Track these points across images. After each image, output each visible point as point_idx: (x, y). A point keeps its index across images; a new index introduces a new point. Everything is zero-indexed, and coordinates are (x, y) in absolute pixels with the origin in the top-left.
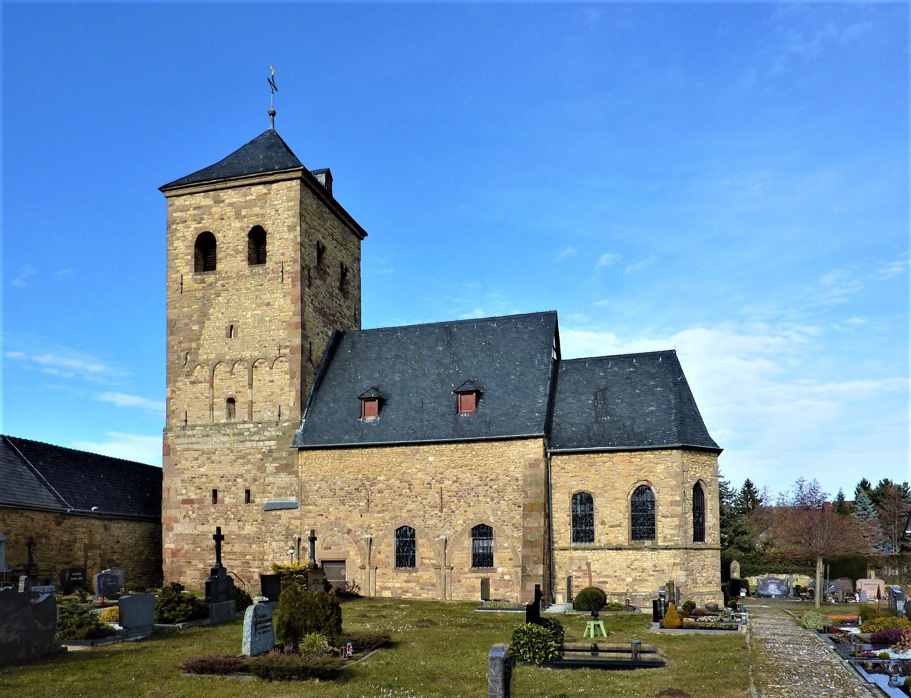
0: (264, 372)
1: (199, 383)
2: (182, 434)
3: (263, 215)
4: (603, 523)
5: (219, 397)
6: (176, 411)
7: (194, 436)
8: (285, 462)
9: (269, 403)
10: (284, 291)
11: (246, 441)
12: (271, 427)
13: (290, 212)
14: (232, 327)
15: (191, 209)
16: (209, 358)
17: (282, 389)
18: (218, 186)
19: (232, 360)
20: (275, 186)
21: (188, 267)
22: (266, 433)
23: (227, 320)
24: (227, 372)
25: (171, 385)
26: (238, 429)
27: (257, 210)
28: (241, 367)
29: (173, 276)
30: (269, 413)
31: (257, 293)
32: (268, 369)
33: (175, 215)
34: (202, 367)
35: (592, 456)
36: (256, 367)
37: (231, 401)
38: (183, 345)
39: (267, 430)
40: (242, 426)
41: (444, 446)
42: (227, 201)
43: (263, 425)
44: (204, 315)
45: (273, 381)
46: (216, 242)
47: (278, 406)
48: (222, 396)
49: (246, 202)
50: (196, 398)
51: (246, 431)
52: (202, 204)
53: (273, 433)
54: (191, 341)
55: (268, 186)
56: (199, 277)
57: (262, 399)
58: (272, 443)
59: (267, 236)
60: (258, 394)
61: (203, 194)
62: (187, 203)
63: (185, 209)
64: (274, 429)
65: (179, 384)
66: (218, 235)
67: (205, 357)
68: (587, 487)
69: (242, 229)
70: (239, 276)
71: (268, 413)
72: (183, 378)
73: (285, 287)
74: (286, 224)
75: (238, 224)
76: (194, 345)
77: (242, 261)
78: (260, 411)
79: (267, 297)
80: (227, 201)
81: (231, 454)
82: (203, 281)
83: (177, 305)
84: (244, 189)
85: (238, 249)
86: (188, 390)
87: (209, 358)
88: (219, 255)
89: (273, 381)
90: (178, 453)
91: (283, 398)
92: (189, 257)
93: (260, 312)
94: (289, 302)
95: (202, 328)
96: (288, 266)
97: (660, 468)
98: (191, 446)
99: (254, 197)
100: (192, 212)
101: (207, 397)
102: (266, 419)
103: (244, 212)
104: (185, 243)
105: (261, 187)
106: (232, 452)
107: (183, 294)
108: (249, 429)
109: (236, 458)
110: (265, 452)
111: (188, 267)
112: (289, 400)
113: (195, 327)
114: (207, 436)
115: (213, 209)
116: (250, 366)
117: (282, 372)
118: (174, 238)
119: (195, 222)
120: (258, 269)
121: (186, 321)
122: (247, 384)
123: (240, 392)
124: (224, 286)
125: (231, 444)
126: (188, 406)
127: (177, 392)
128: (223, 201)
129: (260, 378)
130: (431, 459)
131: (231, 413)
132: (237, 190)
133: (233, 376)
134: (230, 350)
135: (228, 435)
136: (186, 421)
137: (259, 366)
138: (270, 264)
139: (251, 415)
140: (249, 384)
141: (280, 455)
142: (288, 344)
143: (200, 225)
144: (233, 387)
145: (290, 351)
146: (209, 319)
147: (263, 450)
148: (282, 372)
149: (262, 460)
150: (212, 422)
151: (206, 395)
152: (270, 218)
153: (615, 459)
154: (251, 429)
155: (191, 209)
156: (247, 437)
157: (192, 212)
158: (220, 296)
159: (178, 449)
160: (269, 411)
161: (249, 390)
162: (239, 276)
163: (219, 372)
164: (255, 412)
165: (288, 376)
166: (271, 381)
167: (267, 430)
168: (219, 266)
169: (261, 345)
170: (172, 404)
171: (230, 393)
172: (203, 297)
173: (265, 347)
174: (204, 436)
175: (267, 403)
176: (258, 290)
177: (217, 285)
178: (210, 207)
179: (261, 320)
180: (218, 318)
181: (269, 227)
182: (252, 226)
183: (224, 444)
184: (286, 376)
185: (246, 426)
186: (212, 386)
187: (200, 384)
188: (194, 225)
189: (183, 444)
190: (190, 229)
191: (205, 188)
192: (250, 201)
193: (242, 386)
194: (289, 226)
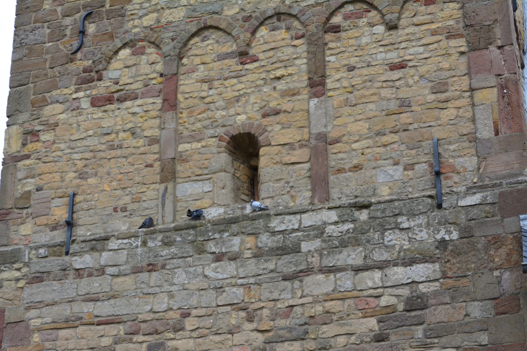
0: (364, 40)
1: (121, 100)
2: (56, 269)
5: (194, 138)
6: (35, 196)
7: (101, 271)
8: (484, 338)
9: (395, 137)
11: (309, 271)
12: (412, 215)
16: (163, 21)
19: (247, 19)
22: (390, 237)
25: (23, 117)
26: (274, 233)
28: (281, 34)
30: (397, 172)
32: (380, 29)
34: (139, 52)
36: (336, 29)
40: (292, 223)
45: (401, 66)
47: (427, 145)
48: (211, 132)
50: (112, 148)
51: (308, 238)
53: (423, 235)
57: (363, 127)
60: (347, 110)
64: (422, 220)
65: (48, 110)
67: (149, 20)
71: (391, 170)
72: (66, 91)
78: (357, 168)
81: (248, 326)
86: (84, 125)
87: (163, 21)
89: (401, 66)
90: (36, 338)
91: (451, 113)
98: (88, 308)
101: (153, 141)
102: (385, 193)
106: (250, 319)
109: (267, 342)
110: (391, 309)
112: (473, 120)
114: (151, 268)
116: (312, 28)
117: (434, 33)
122: (306, 83)
123: (277, 113)
125: (247, 287)
126: (82, 176)
127: (44, 137)
129: (353, 61)
133: (256, 64)
135: (233, 258)
136: (70, 224)
137: (345, 24)
140: (312, 84)
141: (459, 316)
144: (252, 99)
147: (384, 301)
148: (434, 33)
149: (380, 338)
150: (169, 218)
151: (148, 133)
154: (330, 229)
156: (315, 261)
159: (35, 323)
160: (396, 164)
161: (314, 102)
163: (197, 60)
164: (339, 171)
165: (461, 44)
166: (394, 67)
167: (397, 227)
170: (20, 175)
171: (243, 117)
174: (136, 271)
175: (385, 139)
183: (219, 289)
184: (453, 43)
185: (308, 220)
187: (128, 103)
189: (54, 304)
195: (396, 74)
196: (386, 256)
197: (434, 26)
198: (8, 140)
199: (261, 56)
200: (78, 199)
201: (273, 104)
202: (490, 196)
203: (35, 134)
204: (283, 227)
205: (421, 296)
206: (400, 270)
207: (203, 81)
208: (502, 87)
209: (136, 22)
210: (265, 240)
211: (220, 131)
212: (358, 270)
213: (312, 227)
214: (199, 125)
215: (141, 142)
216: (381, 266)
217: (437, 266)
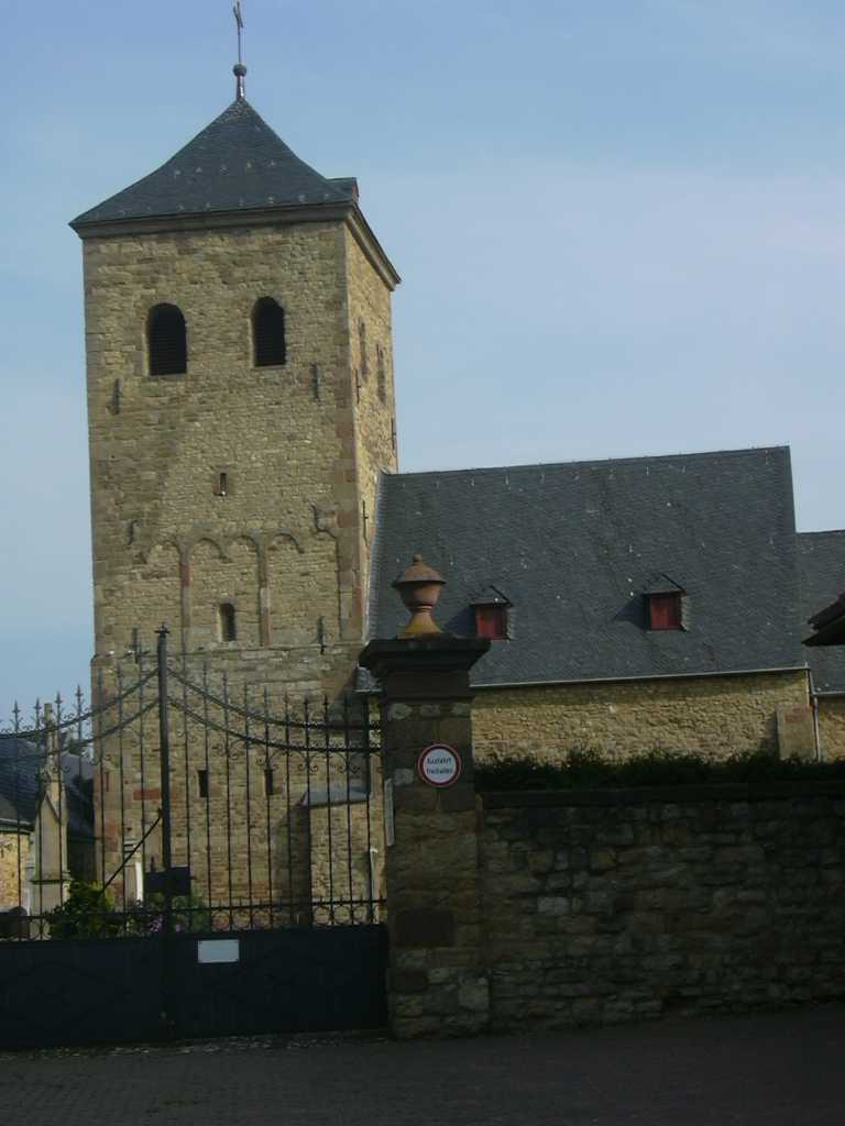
10: (323, 413)
12: (310, 656)
14: (223, 475)
17: (323, 589)
23: (212, 464)
24: (215, 557)
25: (104, 580)
29: (100, 380)
31: (270, 417)
37: (228, 611)
38: (127, 507)
39: (302, 662)
40: (252, 655)
41: (636, 688)
43: (292, 655)
44: (166, 453)
46: (184, 322)
53: (315, 667)
56: (155, 384)
58: (313, 684)
59: (287, 317)
61: (154, 236)
66: (189, 310)
67: (172, 529)
69: (236, 303)
70: (234, 385)
72: (127, 568)
73: (322, 408)
74: (321, 297)
75: (224, 292)
76: (147, 508)
78: (283, 628)
79: (289, 425)
83: (111, 434)
85: (229, 338)
88: (192, 348)
93: (278, 451)
94: (334, 434)
96: (328, 370)
99: (256, 248)
102: (296, 643)
107: (122, 414)
108: (264, 661)
113: (153, 475)
117: (323, 558)
119: (141, 286)
120: (271, 373)
121: (131, 463)
124: (204, 402)
128: (195, 251)
130: (612, 709)
131: (230, 633)
134: (220, 517)
138: (294, 366)
139: (263, 635)
142: (334, 508)
145: (339, 522)
148: (323, 558)
158: (196, 420)
162: (234, 385)
165: (334, 566)
166: (304, 575)
167: (302, 662)
168: (193, 367)
169: (281, 510)
173: (290, 513)
176: (271, 412)
177: (190, 400)
178: (173, 260)
179: (280, 464)
180: (195, 461)
181: (287, 298)
182: (255, 298)
185: (262, 655)
186: (185, 582)
187: (164, 579)
190: (133, 299)
193: (246, 583)
194: (327, 302)
195: (304, 579)
196: (298, 676)
197: (322, 554)
198: (96, 593)
199: (235, 560)
200: (139, 631)
201: (242, 589)
202: (345, 650)
203: (112, 592)
204: (247, 657)
205: (311, 697)
206: (303, 683)
207: (202, 570)
208: (354, 593)
209: (164, 530)
210: (241, 664)
211: (214, 601)
212: (285, 682)
213: (263, 659)
214: (203, 596)
215: (170, 603)
216: (295, 681)
217: (319, 682)
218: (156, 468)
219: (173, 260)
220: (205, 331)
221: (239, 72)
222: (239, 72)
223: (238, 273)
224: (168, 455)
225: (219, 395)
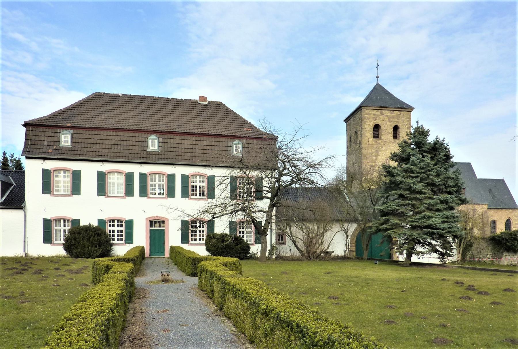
3: (398, 122)
4: (499, 229)
13: (408, 123)
15: (372, 115)
18: (383, 109)
20: (402, 112)
21: (371, 136)
27: (396, 120)
33: (365, 116)
35: (497, 210)
42: (385, 114)
44: (377, 154)
49: (392, 116)
52: (376, 114)
54: (372, 162)
55: (400, 112)
62: (370, 112)
63: (370, 114)
68: (495, 219)
69: (391, 125)
70: (390, 142)
75: (390, 124)
77: (391, 137)
80: (385, 114)
82: (376, 142)
84: (391, 111)
88: (383, 133)
92: (371, 132)
95: (376, 158)
97: (513, 214)
99: (395, 115)
100: (372, 116)
103: (391, 120)
104: (370, 127)
105: (397, 112)
111: (371, 136)
113: (374, 158)
115: (380, 116)
118: (365, 124)
128: (384, 114)
132: (389, 112)
143: (375, 121)
146: (379, 156)
152: (401, 123)
153: (502, 211)
155: (372, 115)
157: (372, 116)
162: (390, 142)
168: (382, 137)
172: (377, 148)
178: (380, 115)
180: (383, 156)
181: (400, 126)
188: (373, 121)
191: (378, 108)
192: (393, 116)
218: (375, 156)
219: (380, 115)
220: (385, 131)
221: (377, 77)
222: (377, 77)
223: (391, 120)
224: (378, 154)
225: (387, 143)
